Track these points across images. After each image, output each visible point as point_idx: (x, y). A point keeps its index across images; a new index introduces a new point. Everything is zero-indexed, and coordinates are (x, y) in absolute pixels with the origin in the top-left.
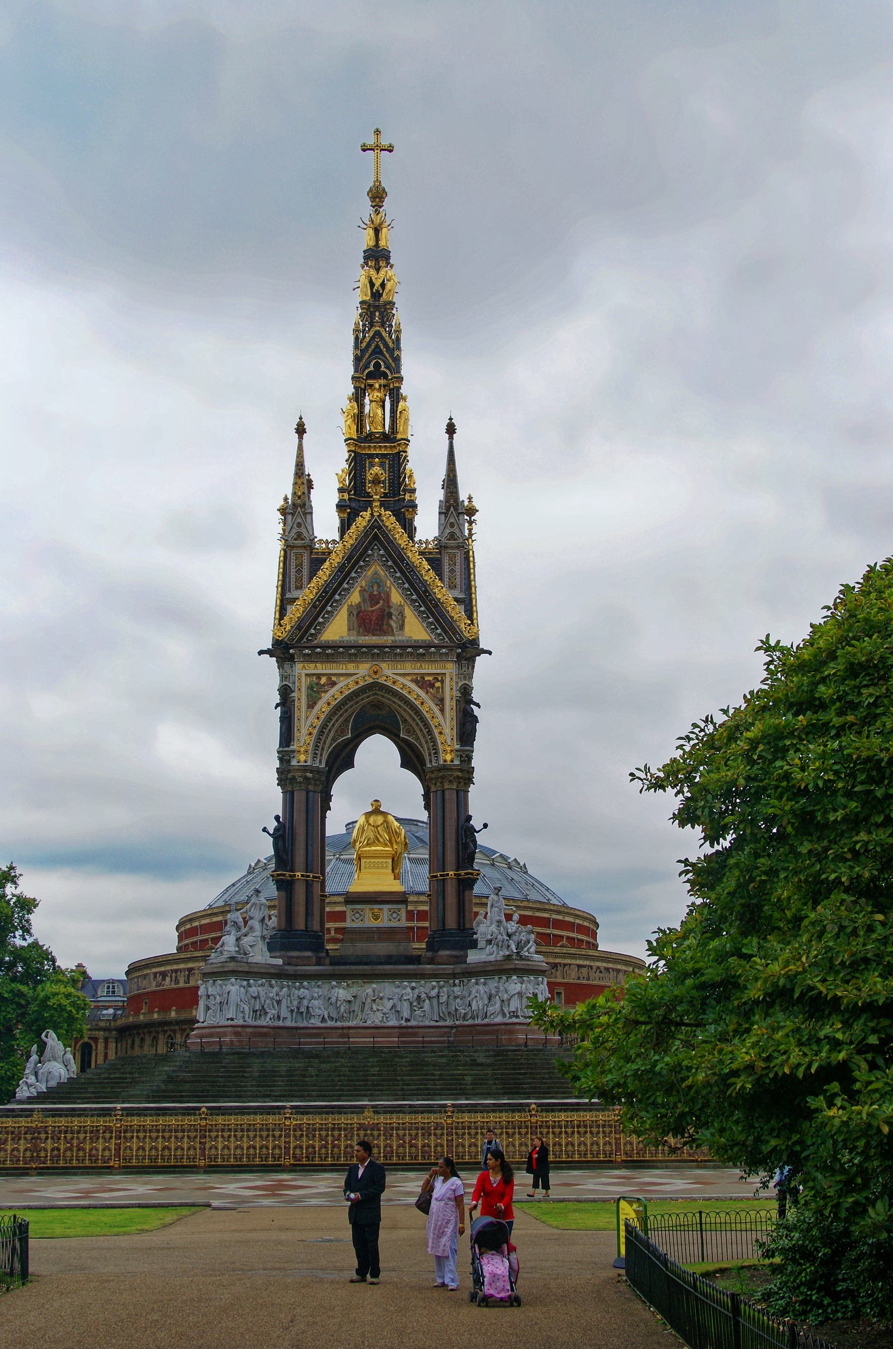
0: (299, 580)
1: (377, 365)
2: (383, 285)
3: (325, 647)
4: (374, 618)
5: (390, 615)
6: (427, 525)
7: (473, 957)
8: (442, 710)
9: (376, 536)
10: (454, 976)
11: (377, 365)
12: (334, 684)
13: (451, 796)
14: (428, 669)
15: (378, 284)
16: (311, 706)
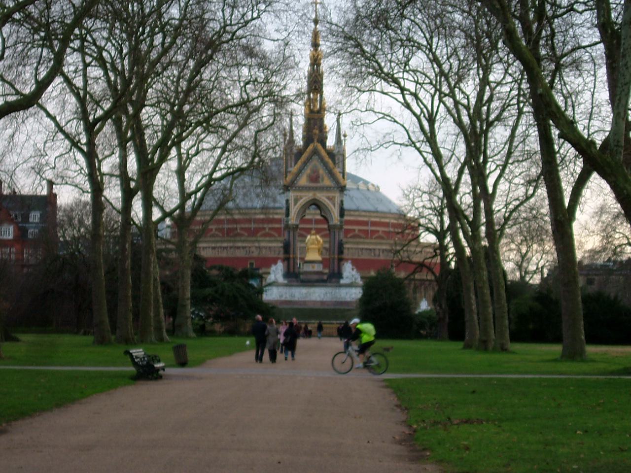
0: (291, 164)
1: (315, 87)
2: (318, 56)
3: (299, 187)
4: (314, 178)
5: (319, 177)
6: (331, 142)
7: (342, 282)
8: (335, 207)
9: (315, 152)
10: (337, 287)
11: (315, 87)
12: (301, 198)
13: (337, 234)
14: (331, 195)
15: (316, 55)
16: (295, 204)
